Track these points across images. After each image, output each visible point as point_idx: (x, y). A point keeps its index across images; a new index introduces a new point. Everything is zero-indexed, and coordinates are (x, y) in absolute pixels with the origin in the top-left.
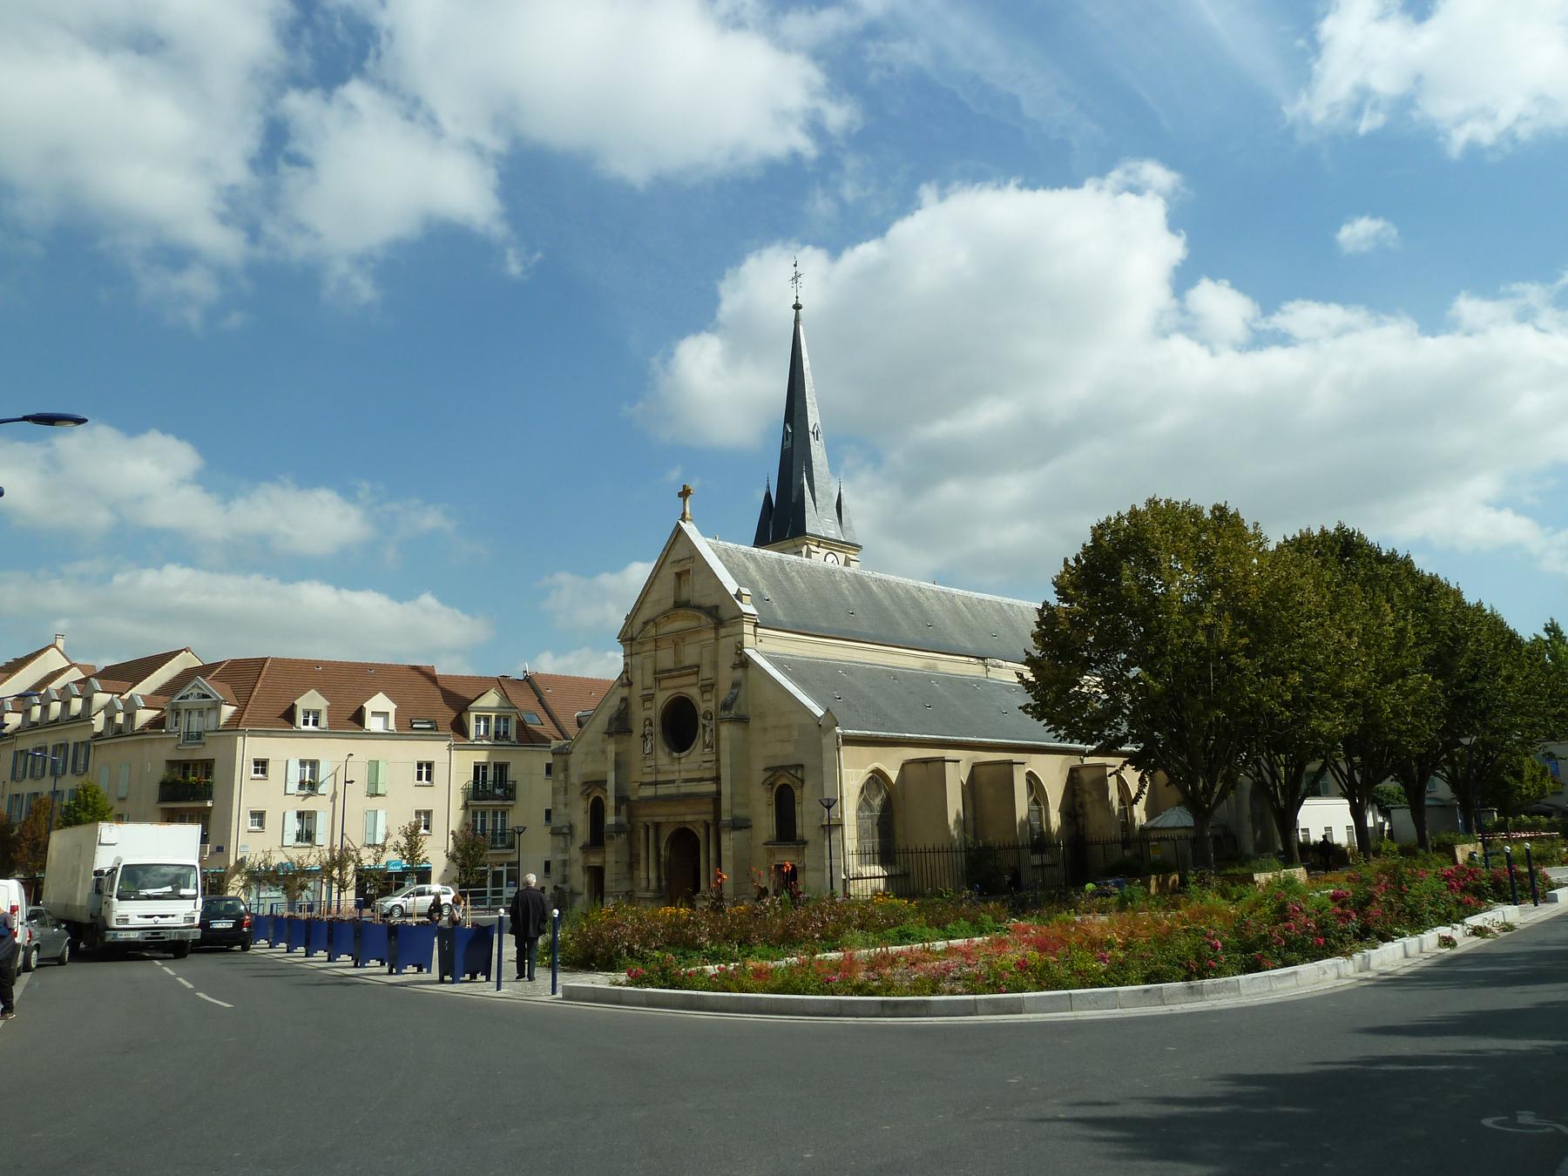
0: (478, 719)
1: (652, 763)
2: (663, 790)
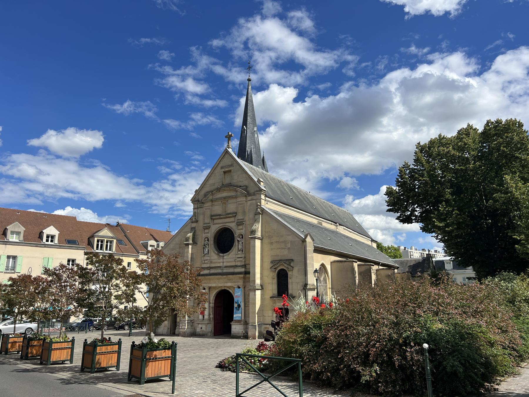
0: (98, 241)
1: (208, 258)
2: (212, 271)
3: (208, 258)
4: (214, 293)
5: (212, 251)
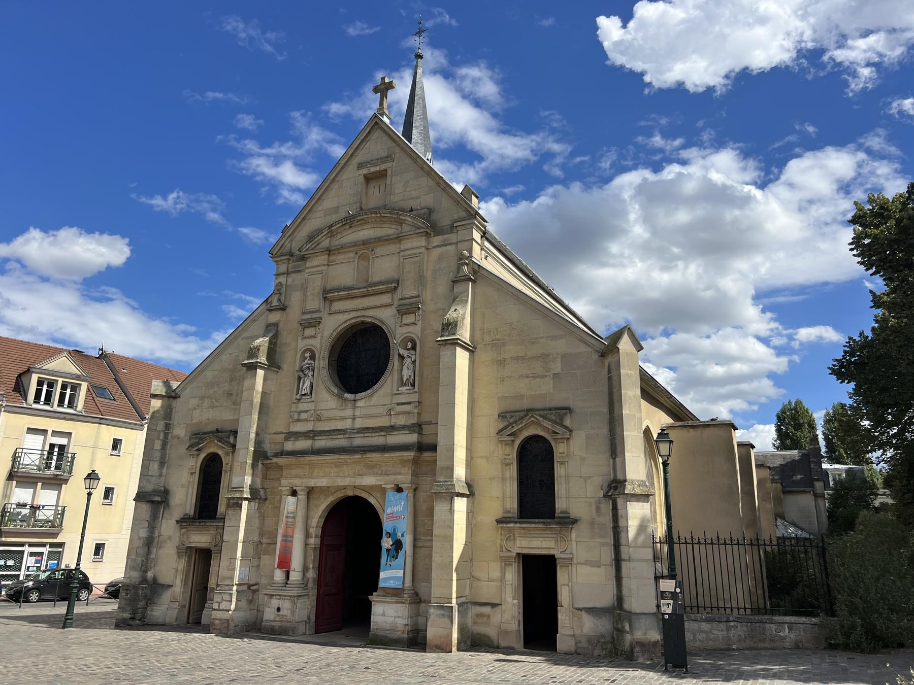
0: (40, 383)
1: (311, 406)
2: (321, 443)
3: (311, 406)
4: (323, 506)
5: (322, 386)
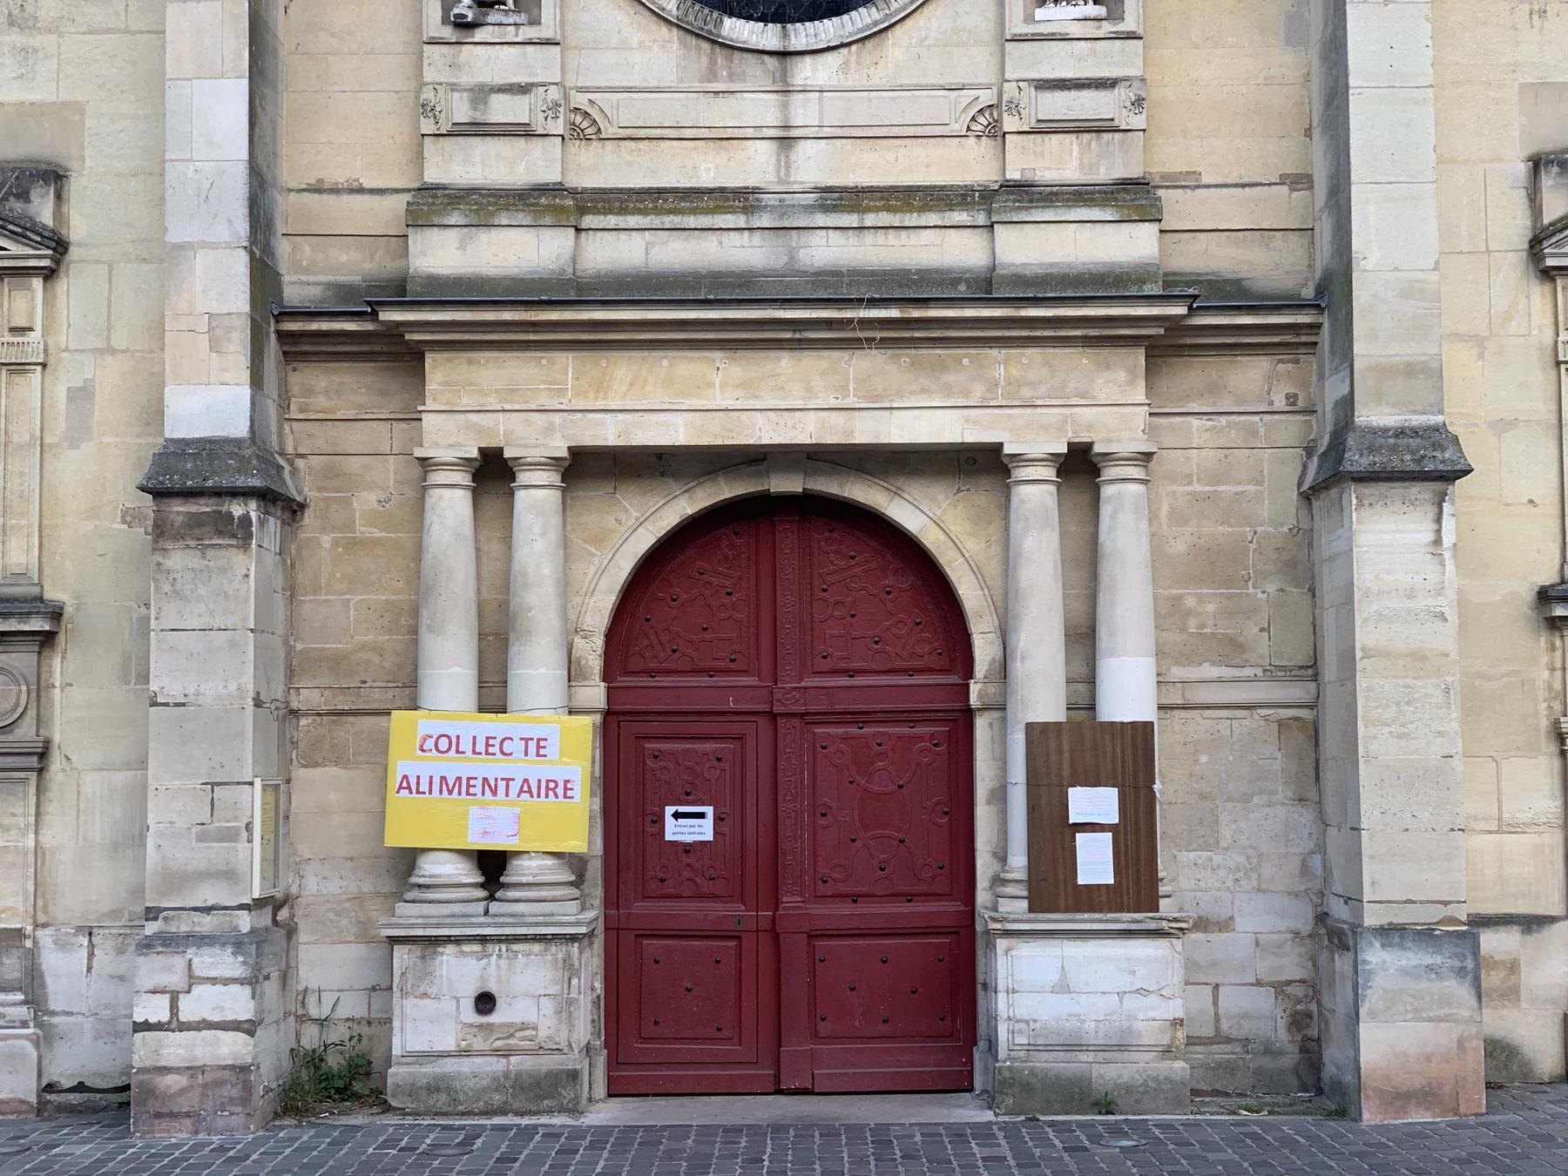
1: (539, 65)
2: (617, 249)
3: (539, 65)
4: (644, 541)
